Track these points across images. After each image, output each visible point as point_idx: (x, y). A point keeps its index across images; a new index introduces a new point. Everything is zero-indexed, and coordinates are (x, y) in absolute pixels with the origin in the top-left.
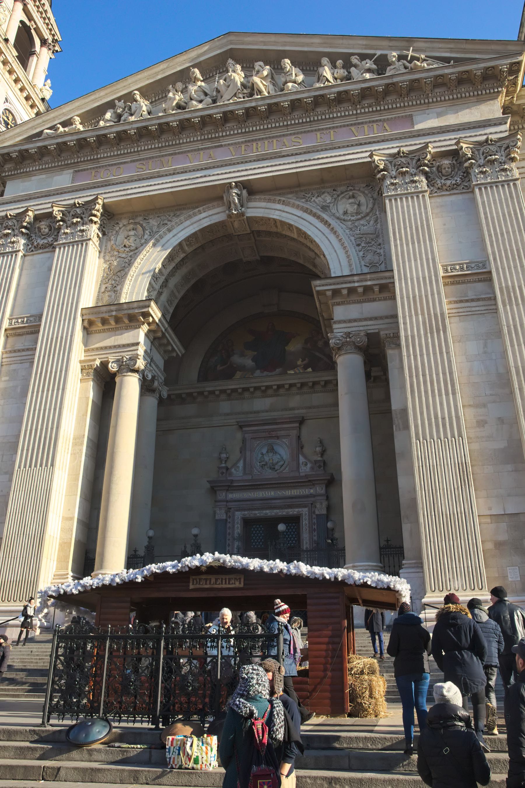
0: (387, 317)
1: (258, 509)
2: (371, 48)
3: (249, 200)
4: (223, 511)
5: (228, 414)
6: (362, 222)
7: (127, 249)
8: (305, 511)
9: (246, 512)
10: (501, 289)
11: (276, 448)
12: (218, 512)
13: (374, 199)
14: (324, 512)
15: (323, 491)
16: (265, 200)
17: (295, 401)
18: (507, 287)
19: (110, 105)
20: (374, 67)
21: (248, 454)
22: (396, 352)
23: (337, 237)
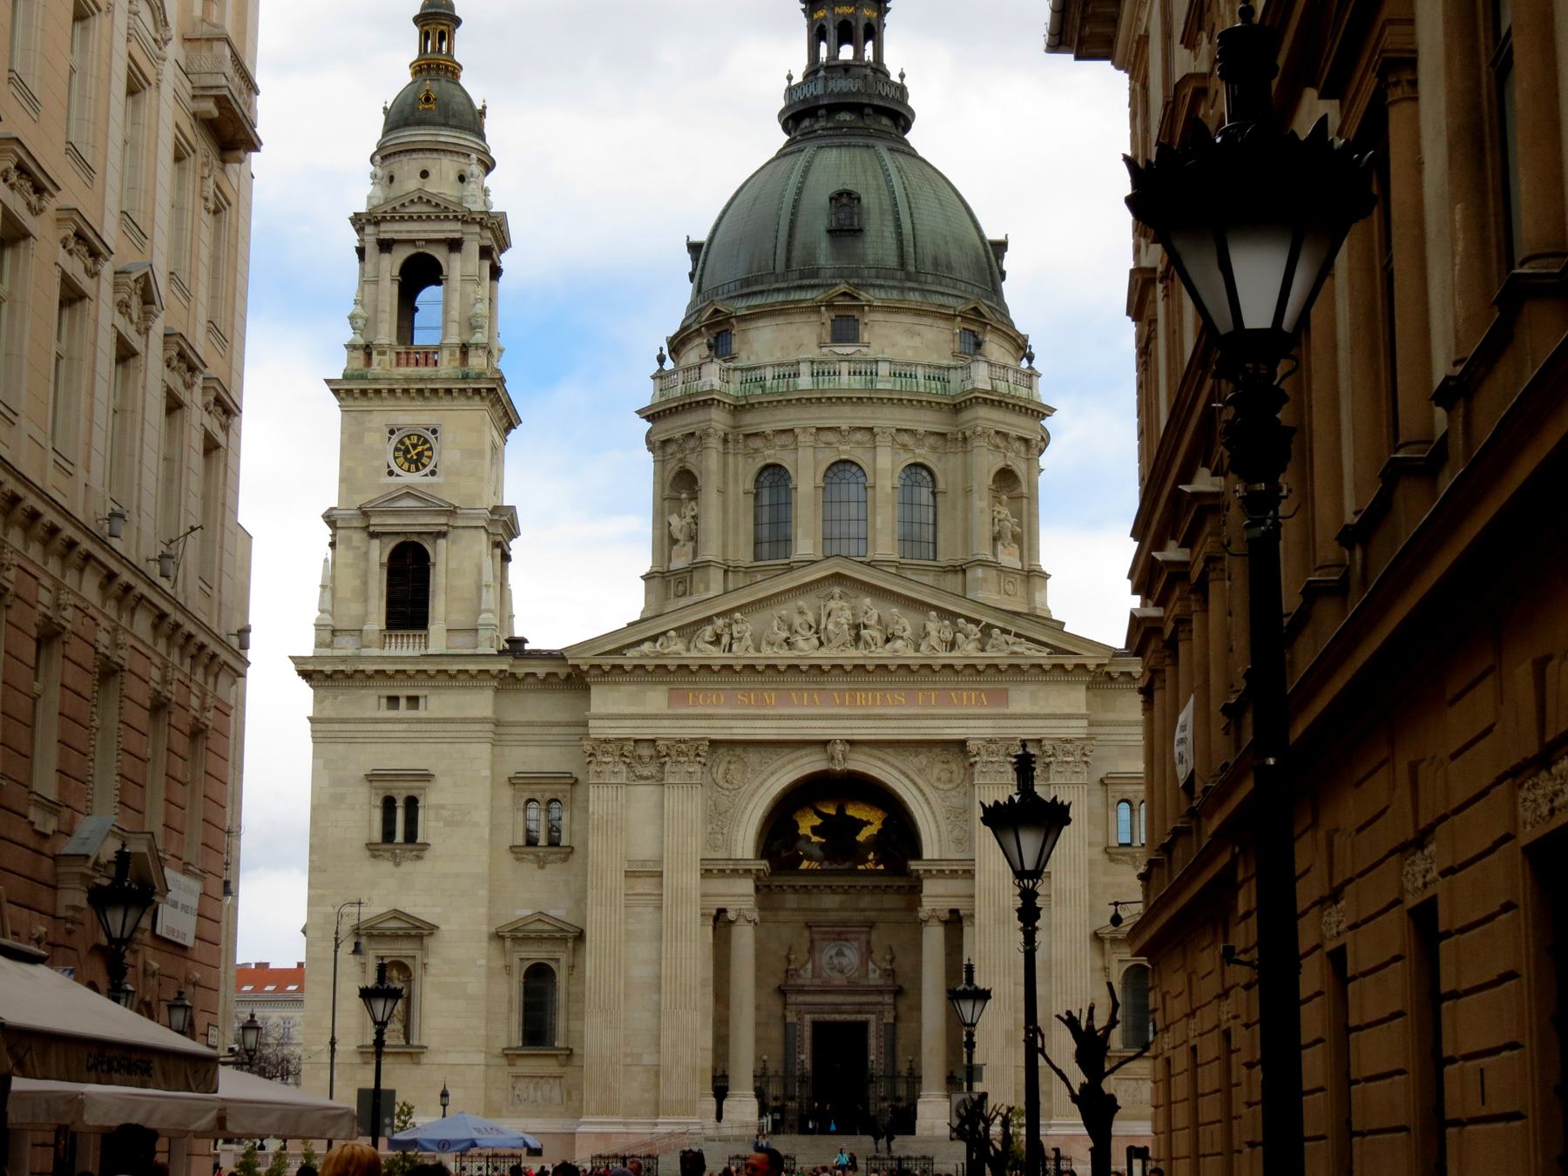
0: (966, 896)
1: (828, 1013)
2: (978, 613)
3: (850, 751)
4: (794, 1014)
5: (793, 910)
6: (953, 793)
7: (730, 787)
8: (872, 1017)
9: (816, 1016)
10: (1056, 891)
11: (847, 952)
12: (788, 1014)
13: (965, 769)
14: (892, 1021)
15: (891, 1001)
16: (866, 754)
17: (866, 901)
18: (1061, 889)
19: (709, 620)
20: (979, 635)
21: (817, 955)
22: (971, 928)
23: (931, 808)
